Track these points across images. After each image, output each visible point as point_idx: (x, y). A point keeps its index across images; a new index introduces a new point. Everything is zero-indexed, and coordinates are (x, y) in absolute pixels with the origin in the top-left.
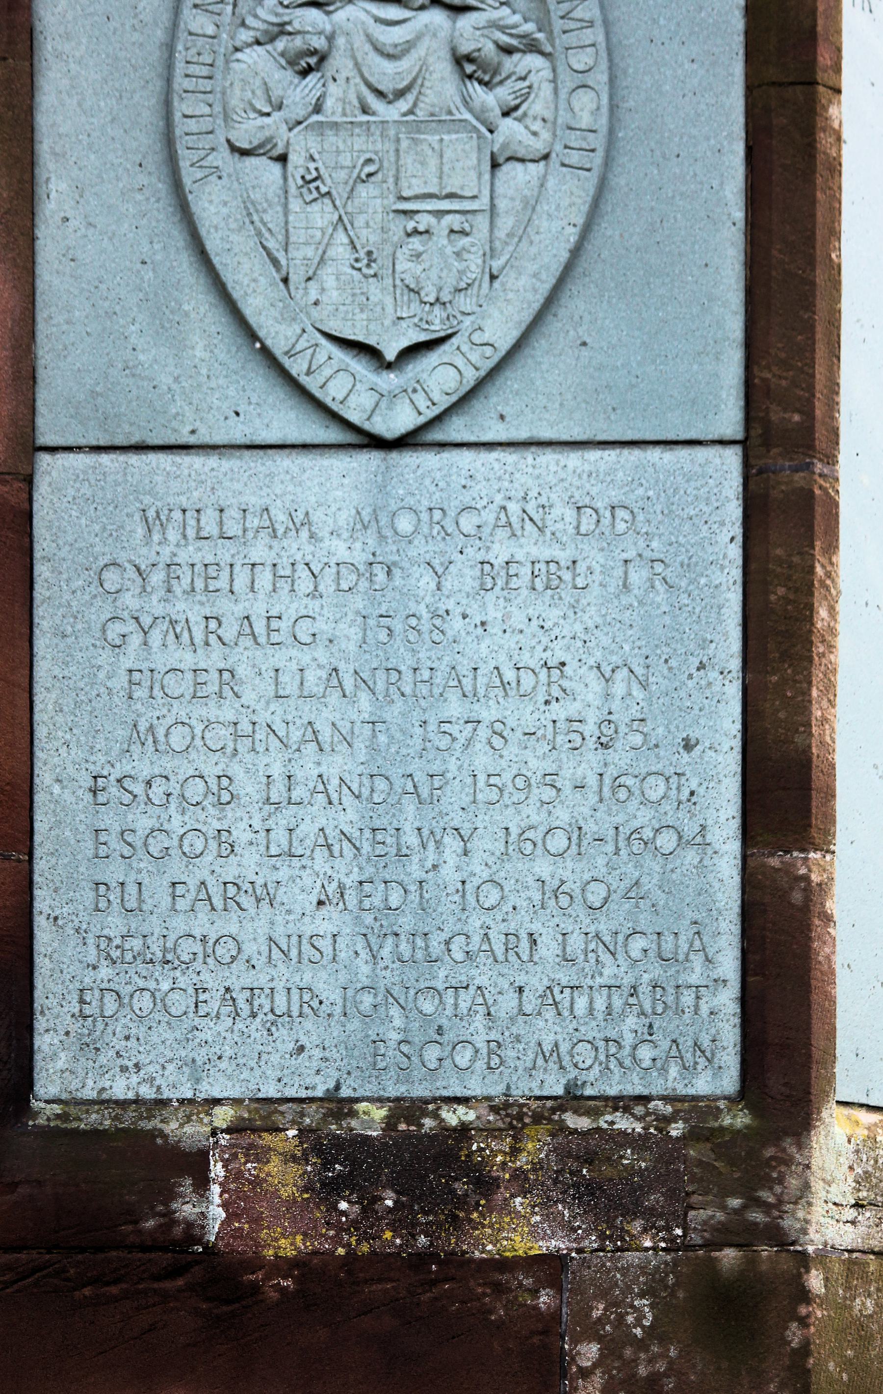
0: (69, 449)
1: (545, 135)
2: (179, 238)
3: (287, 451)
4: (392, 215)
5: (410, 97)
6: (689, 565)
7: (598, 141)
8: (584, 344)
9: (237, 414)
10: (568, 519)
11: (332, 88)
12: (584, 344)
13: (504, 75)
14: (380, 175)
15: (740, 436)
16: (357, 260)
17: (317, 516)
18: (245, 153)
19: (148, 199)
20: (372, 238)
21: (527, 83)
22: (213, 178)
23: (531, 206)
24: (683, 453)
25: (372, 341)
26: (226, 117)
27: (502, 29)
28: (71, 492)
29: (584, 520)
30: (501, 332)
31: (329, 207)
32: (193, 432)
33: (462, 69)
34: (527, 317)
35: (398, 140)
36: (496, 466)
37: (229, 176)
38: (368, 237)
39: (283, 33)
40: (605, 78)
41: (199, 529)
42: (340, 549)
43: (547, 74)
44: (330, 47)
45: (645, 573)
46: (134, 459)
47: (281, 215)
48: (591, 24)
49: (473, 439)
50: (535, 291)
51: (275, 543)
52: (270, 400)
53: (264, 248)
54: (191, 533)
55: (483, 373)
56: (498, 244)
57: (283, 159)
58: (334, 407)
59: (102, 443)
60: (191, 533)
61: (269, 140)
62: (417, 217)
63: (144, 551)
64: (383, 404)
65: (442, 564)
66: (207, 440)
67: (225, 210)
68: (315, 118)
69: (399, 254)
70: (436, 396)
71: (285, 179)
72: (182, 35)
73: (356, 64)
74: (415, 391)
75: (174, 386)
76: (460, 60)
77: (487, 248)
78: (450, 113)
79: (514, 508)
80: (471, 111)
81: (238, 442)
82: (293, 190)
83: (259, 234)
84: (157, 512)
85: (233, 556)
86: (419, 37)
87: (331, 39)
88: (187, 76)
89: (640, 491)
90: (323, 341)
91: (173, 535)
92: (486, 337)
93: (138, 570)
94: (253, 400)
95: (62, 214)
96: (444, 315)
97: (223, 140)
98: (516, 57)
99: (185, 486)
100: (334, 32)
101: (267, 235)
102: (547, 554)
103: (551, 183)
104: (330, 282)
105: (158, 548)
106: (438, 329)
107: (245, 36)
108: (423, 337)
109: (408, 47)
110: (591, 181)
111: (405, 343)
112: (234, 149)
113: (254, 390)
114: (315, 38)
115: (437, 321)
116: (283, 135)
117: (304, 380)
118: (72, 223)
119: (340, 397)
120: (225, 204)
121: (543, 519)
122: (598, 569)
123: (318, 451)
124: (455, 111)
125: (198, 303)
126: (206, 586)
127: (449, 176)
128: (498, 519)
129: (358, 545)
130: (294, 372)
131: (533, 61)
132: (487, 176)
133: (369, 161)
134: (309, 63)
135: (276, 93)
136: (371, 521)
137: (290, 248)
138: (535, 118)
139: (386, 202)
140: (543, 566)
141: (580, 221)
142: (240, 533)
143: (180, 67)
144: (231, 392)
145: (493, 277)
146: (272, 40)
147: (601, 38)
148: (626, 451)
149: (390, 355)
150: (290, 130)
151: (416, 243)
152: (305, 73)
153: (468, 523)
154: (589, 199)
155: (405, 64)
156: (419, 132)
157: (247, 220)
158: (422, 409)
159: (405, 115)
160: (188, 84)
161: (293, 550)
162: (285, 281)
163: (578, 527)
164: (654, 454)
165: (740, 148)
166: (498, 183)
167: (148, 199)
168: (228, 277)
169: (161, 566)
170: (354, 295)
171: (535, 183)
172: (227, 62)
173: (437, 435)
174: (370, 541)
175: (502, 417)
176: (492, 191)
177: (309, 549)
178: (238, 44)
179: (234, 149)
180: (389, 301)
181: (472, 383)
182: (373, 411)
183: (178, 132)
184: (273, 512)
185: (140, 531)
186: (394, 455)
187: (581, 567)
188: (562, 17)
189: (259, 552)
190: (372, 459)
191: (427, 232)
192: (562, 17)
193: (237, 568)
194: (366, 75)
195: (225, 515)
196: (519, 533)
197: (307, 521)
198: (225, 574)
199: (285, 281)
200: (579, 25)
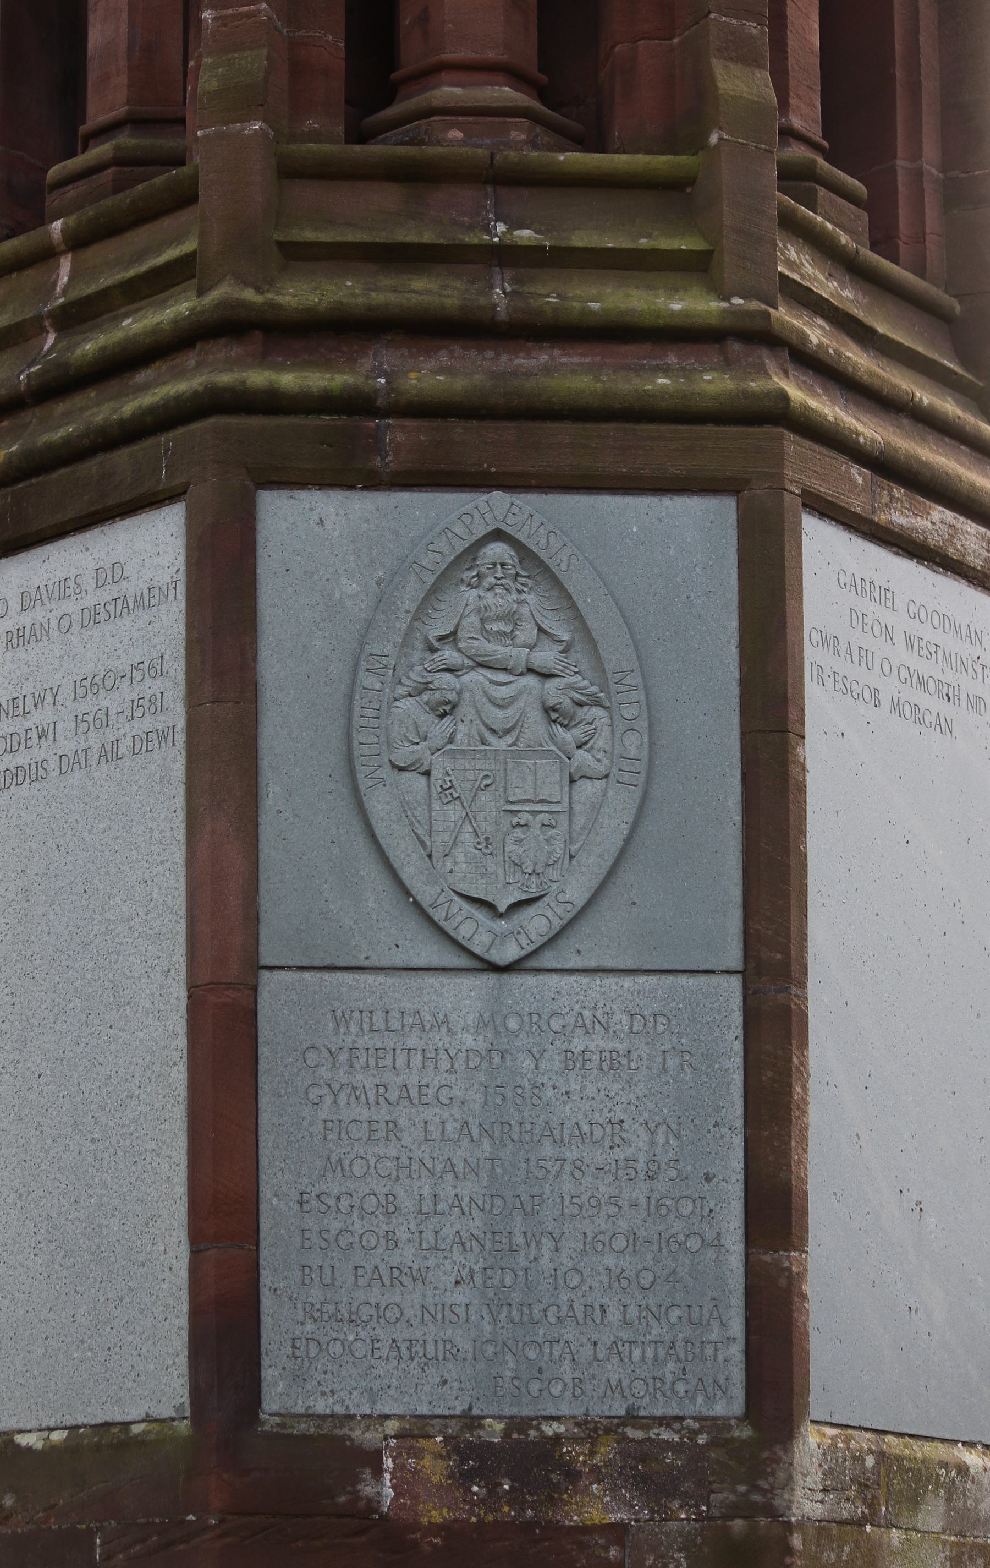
0: (282, 968)
1: (606, 761)
2: (356, 826)
3: (431, 972)
4: (502, 813)
5: (514, 734)
6: (707, 1055)
7: (642, 767)
8: (634, 903)
9: (398, 946)
10: (624, 1023)
11: (461, 727)
12: (634, 903)
13: (577, 721)
14: (494, 786)
15: (740, 968)
16: (478, 843)
17: (453, 1017)
18: (401, 769)
19: (335, 799)
20: (489, 829)
21: (593, 727)
22: (380, 786)
23: (597, 809)
24: (703, 979)
25: (489, 898)
26: (389, 744)
27: (576, 690)
28: (283, 997)
29: (635, 1023)
30: (577, 893)
31: (459, 807)
32: (367, 958)
33: (549, 716)
34: (595, 884)
35: (506, 763)
36: (575, 985)
37: (391, 784)
38: (487, 828)
39: (427, 689)
40: (646, 724)
41: (372, 1025)
42: (469, 1040)
43: (606, 720)
44: (459, 700)
45: (677, 1060)
46: (327, 976)
47: (426, 812)
48: (636, 688)
49: (559, 966)
50: (601, 867)
51: (424, 1035)
52: (420, 937)
53: (415, 834)
54: (366, 1027)
55: (565, 922)
56: (574, 834)
57: (427, 774)
58: (464, 943)
59: (304, 964)
60: (366, 1027)
61: (418, 760)
62: (520, 815)
63: (334, 1039)
64: (497, 942)
65: (539, 1051)
66: (377, 964)
67: (388, 808)
68: (450, 746)
69: (507, 840)
70: (533, 937)
71: (429, 787)
72: (359, 689)
73: (477, 711)
74: (519, 933)
75: (354, 927)
76: (548, 710)
77: (567, 837)
78: (541, 745)
79: (587, 1013)
80: (555, 744)
81: (398, 966)
82: (434, 795)
83: (412, 824)
84: (343, 1013)
85: (395, 1043)
86: (520, 693)
87: (459, 693)
88: (362, 716)
89: (673, 1004)
90: (456, 898)
91: (354, 1029)
92: (567, 897)
93: (330, 1052)
94: (408, 937)
95: (277, 808)
96: (539, 882)
97: (386, 760)
98: (586, 708)
99: (362, 995)
100: (462, 689)
101: (417, 825)
102: (611, 1046)
103: (610, 793)
104: (461, 858)
105: (343, 1037)
106: (534, 891)
107: (401, 690)
108: (524, 897)
109: (512, 700)
110: (637, 793)
111: (512, 901)
112: (394, 766)
113: (408, 930)
114: (449, 693)
115: (534, 886)
116: (427, 758)
117: (443, 924)
118: (284, 815)
119: (468, 936)
120: (389, 803)
121: (607, 1022)
122: (645, 1056)
123: (453, 973)
124: (544, 744)
125: (370, 870)
126: (377, 1064)
127: (541, 788)
128: (577, 1021)
129: (481, 1038)
130: (436, 919)
131: (597, 712)
132: (567, 789)
133: (486, 776)
134: (446, 710)
135: (423, 730)
136: (490, 1021)
137: (433, 834)
138: (599, 750)
139: (498, 804)
140: (608, 1054)
141: (630, 820)
142: (400, 1028)
143: (357, 711)
144: (393, 931)
145: (571, 857)
146: (420, 694)
147: (643, 697)
148: (663, 977)
149: (502, 908)
150: (432, 754)
151: (518, 832)
152: (443, 716)
153: (556, 1024)
154: (636, 805)
155: (510, 712)
156: (520, 758)
157: (403, 815)
158: (524, 945)
159: (510, 746)
160: (363, 722)
161: (437, 1040)
162: (430, 856)
163: (631, 1028)
164: (683, 980)
165: (738, 774)
166: (574, 793)
167: (335, 799)
168: (390, 853)
169: (346, 1049)
170: (477, 867)
171: (599, 793)
172: (389, 708)
173: (533, 963)
174: (489, 1035)
175: (579, 952)
176: (570, 798)
177: (447, 1039)
178: (397, 696)
179: (394, 766)
180: (500, 871)
181: (558, 928)
182: (491, 946)
183: (356, 754)
184: (422, 1014)
185: (331, 1025)
186: (505, 977)
187: (634, 1056)
188: (616, 683)
189: (412, 1042)
190: (490, 979)
191: (526, 825)
192: (616, 683)
193: (398, 1052)
194: (484, 718)
195: (390, 1015)
196: (591, 1031)
197: (446, 1020)
198: (390, 1056)
199: (430, 856)
200: (628, 688)
